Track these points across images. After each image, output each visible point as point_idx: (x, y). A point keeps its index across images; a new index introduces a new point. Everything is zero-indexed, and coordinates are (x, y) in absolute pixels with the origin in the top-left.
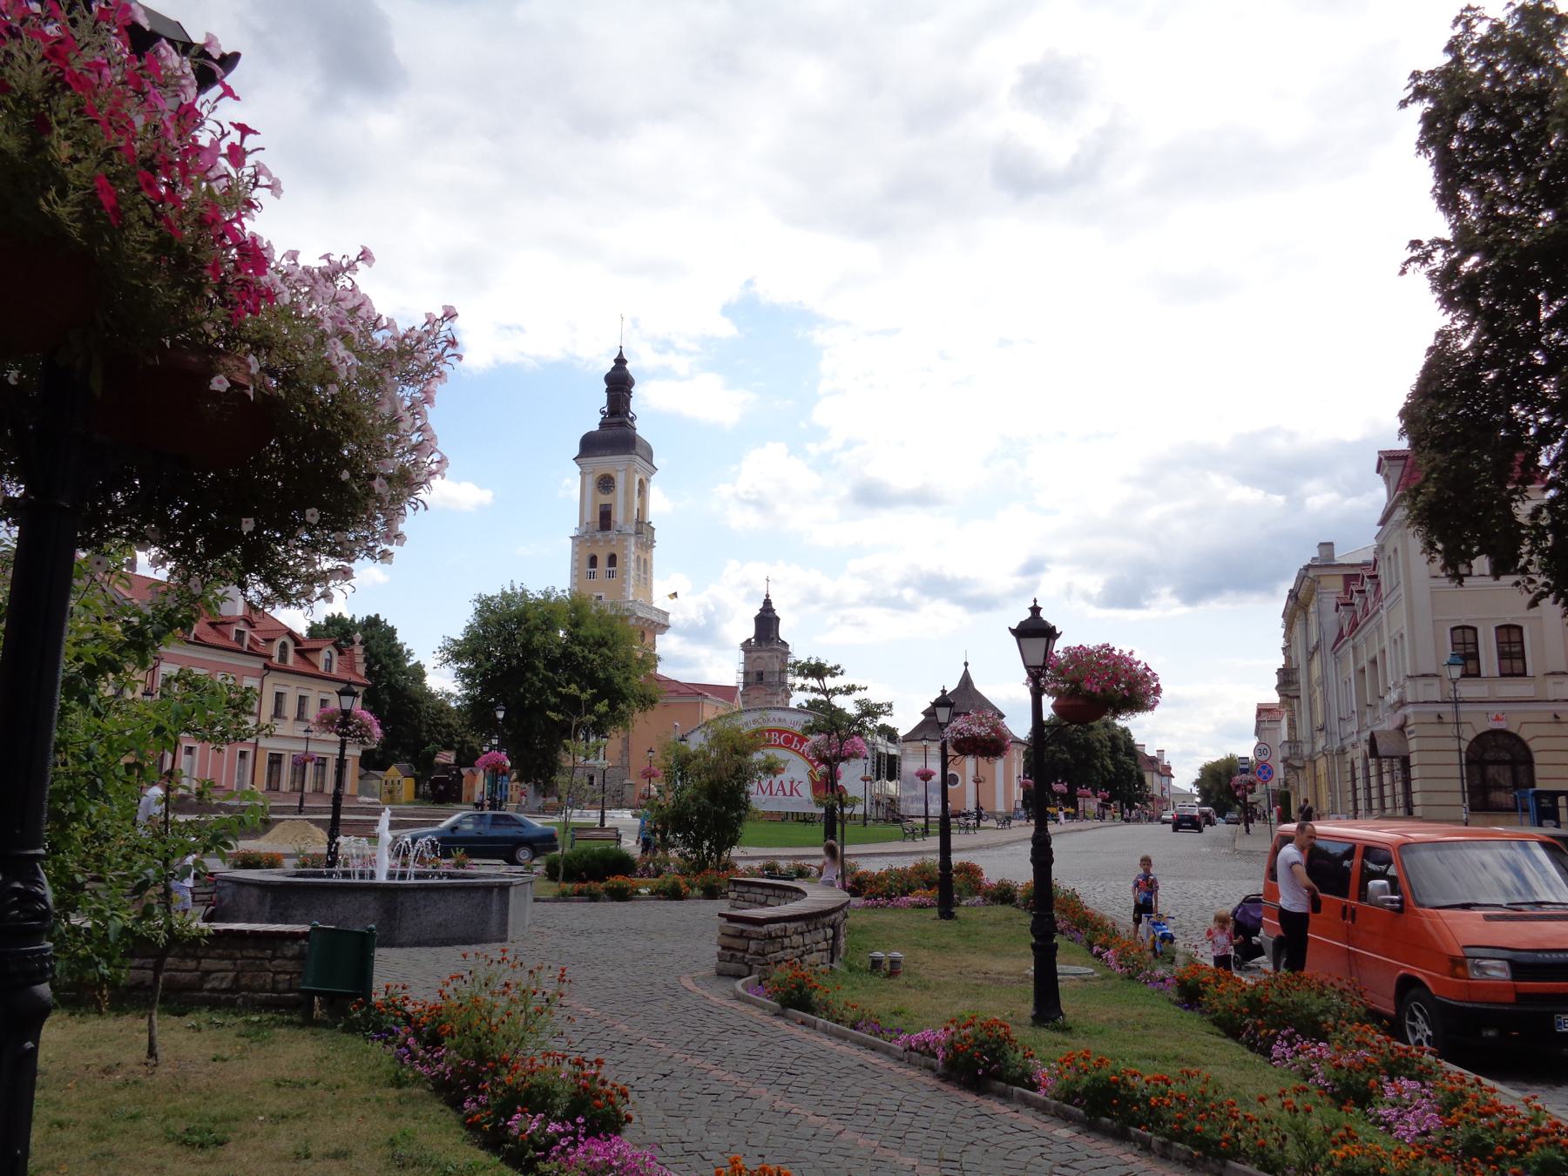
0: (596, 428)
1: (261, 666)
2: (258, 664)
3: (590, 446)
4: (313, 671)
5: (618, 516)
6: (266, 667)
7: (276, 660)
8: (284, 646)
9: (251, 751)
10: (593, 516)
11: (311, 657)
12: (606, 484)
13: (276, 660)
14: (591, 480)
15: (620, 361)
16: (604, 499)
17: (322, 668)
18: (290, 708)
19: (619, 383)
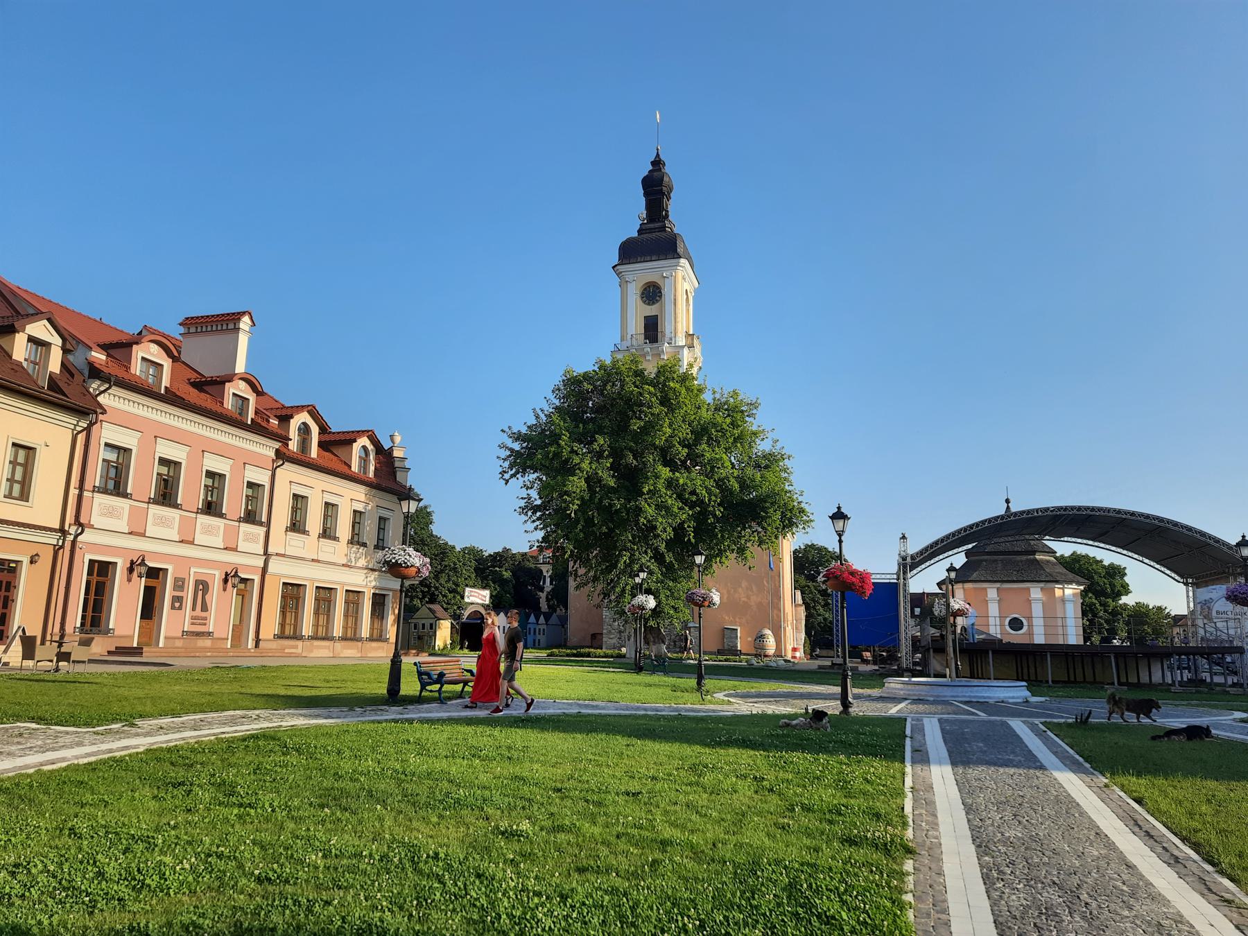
0: (636, 235)
1: (272, 454)
2: (267, 448)
3: (630, 252)
4: (344, 469)
5: (666, 327)
7: (293, 446)
8: (305, 429)
9: (257, 579)
10: (636, 327)
11: (340, 451)
12: (652, 293)
13: (293, 446)
14: (634, 291)
15: (657, 163)
16: (651, 310)
17: (355, 467)
18: (314, 521)
19: (655, 188)
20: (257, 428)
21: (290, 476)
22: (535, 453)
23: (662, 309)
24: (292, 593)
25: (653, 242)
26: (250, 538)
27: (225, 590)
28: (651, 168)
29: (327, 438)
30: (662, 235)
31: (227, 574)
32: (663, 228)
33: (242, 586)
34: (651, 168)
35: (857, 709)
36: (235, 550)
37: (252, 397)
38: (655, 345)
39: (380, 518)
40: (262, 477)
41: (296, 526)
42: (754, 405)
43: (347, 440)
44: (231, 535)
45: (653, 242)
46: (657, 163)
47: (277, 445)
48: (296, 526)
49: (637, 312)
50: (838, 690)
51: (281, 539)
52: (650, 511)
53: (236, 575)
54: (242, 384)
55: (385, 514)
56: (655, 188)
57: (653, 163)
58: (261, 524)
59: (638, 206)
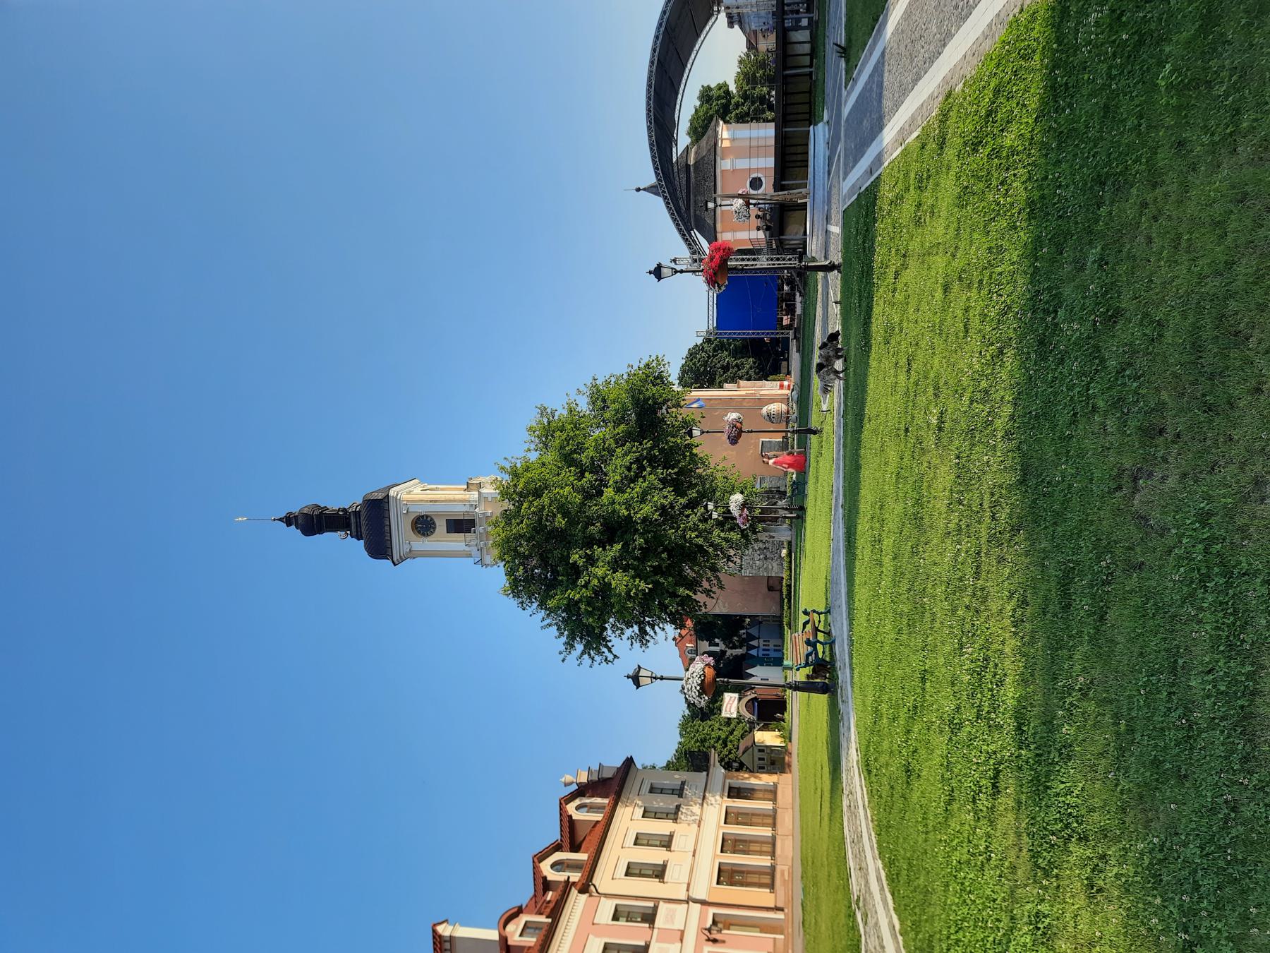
0: (362, 542)
1: (584, 897)
2: (577, 902)
3: (380, 547)
4: (599, 829)
5: (459, 510)
6: (584, 889)
7: (575, 877)
9: (712, 911)
10: (458, 542)
11: (581, 833)
12: (423, 525)
13: (575, 877)
15: (289, 520)
16: (441, 526)
17: (598, 817)
18: (654, 856)
19: (315, 522)
20: (556, 912)
21: (609, 876)
22: (586, 628)
23: (439, 515)
24: (726, 875)
25: (371, 524)
26: (671, 918)
27: (724, 942)
28: (293, 527)
29: (566, 844)
30: (363, 514)
31: (708, 940)
32: (357, 514)
33: (720, 925)
34: (293, 527)
35: (837, 258)
36: (682, 932)
37: (524, 918)
38: (477, 521)
39: (651, 792)
40: (607, 907)
41: (659, 872)
42: (543, 411)
43: (570, 826)
44: (666, 936)
45: (371, 524)
46: (289, 520)
47: (574, 892)
48: (659, 872)
49: (443, 540)
50: (820, 275)
51: (673, 886)
52: (647, 509)
53: (709, 930)
54: (510, 927)
55: (646, 787)
56: (315, 522)
57: (289, 525)
58: (656, 908)
59: (332, 540)
